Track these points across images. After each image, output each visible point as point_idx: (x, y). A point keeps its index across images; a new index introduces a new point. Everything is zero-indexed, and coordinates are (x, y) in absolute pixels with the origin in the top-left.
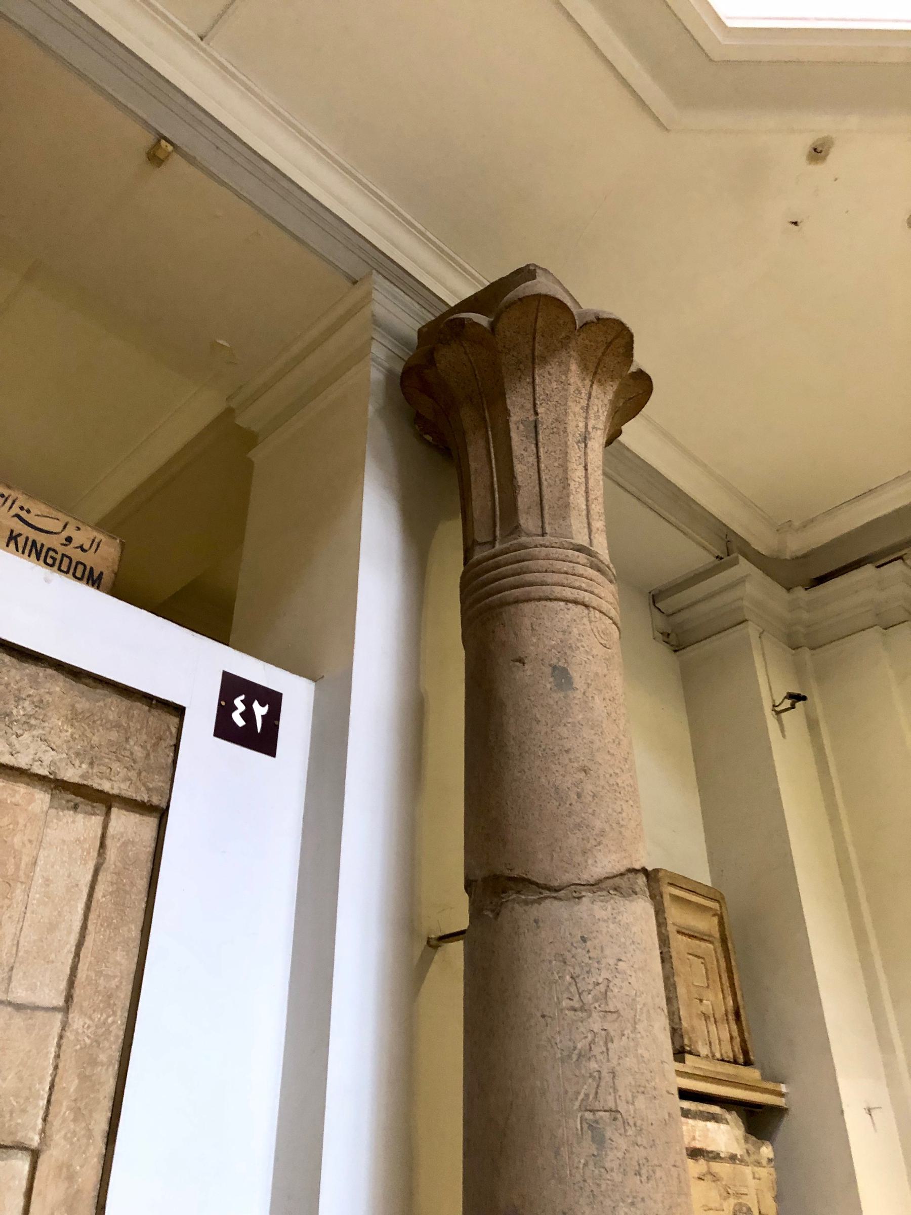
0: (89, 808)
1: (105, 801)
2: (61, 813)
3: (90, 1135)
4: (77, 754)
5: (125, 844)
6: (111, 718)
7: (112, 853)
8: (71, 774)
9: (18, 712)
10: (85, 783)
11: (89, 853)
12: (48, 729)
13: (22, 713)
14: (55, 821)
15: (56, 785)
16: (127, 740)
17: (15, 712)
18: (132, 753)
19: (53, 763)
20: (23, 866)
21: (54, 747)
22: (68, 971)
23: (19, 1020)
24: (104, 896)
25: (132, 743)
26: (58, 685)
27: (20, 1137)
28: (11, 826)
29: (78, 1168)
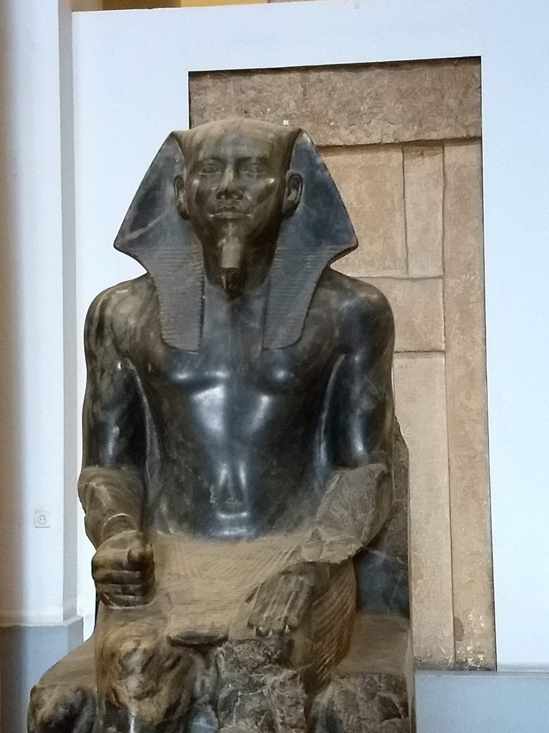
0: (432, 152)
1: (440, 144)
2: (414, 161)
3: (473, 340)
4: (409, 121)
5: (459, 168)
6: (427, 86)
7: (451, 178)
8: (407, 136)
9: (364, 108)
10: (419, 139)
11: (438, 181)
12: (385, 112)
13: (366, 107)
14: (412, 167)
15: (403, 146)
16: (443, 98)
17: (362, 109)
18: (448, 106)
19: (395, 132)
20: (396, 200)
21: (393, 122)
22: (441, 255)
23: (416, 286)
24: (451, 206)
25: (446, 98)
26: (385, 78)
27: (433, 345)
28: (383, 180)
29: (470, 358)
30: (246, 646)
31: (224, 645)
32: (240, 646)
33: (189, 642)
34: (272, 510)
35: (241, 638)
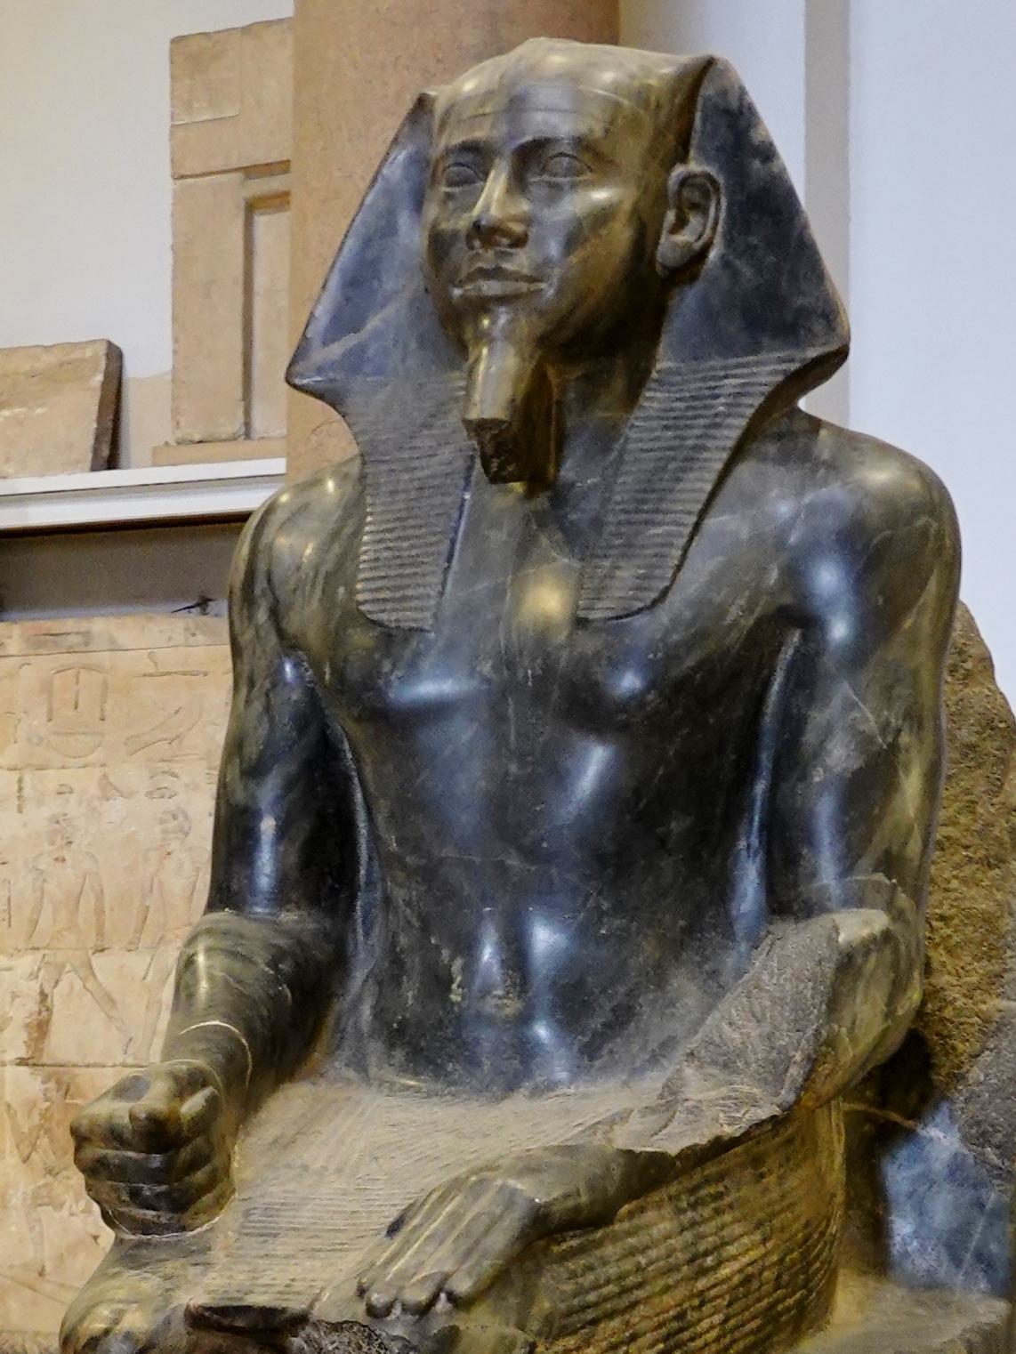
30: (346, 1336)
31: (303, 1334)
32: (335, 1337)
33: (226, 1322)
34: (596, 1023)
35: (334, 1317)
